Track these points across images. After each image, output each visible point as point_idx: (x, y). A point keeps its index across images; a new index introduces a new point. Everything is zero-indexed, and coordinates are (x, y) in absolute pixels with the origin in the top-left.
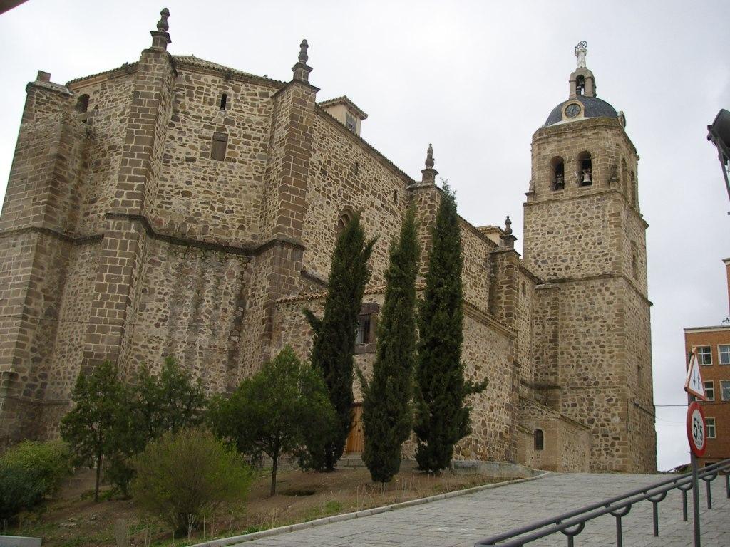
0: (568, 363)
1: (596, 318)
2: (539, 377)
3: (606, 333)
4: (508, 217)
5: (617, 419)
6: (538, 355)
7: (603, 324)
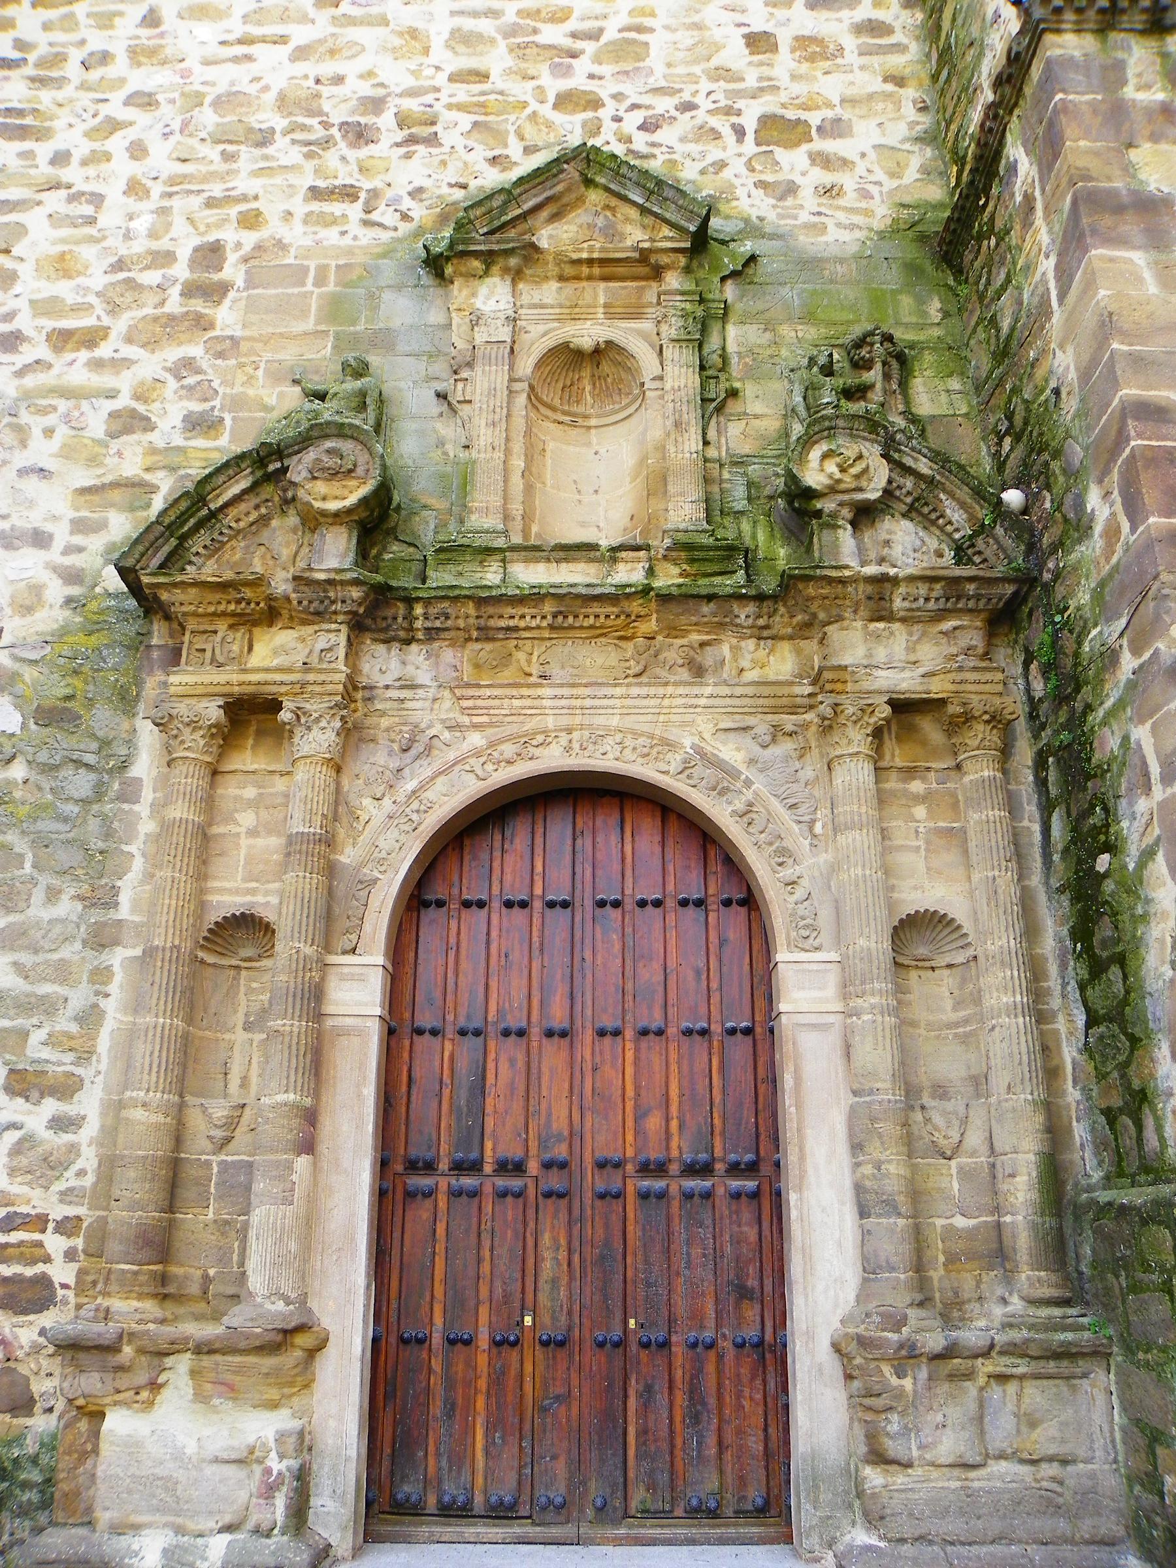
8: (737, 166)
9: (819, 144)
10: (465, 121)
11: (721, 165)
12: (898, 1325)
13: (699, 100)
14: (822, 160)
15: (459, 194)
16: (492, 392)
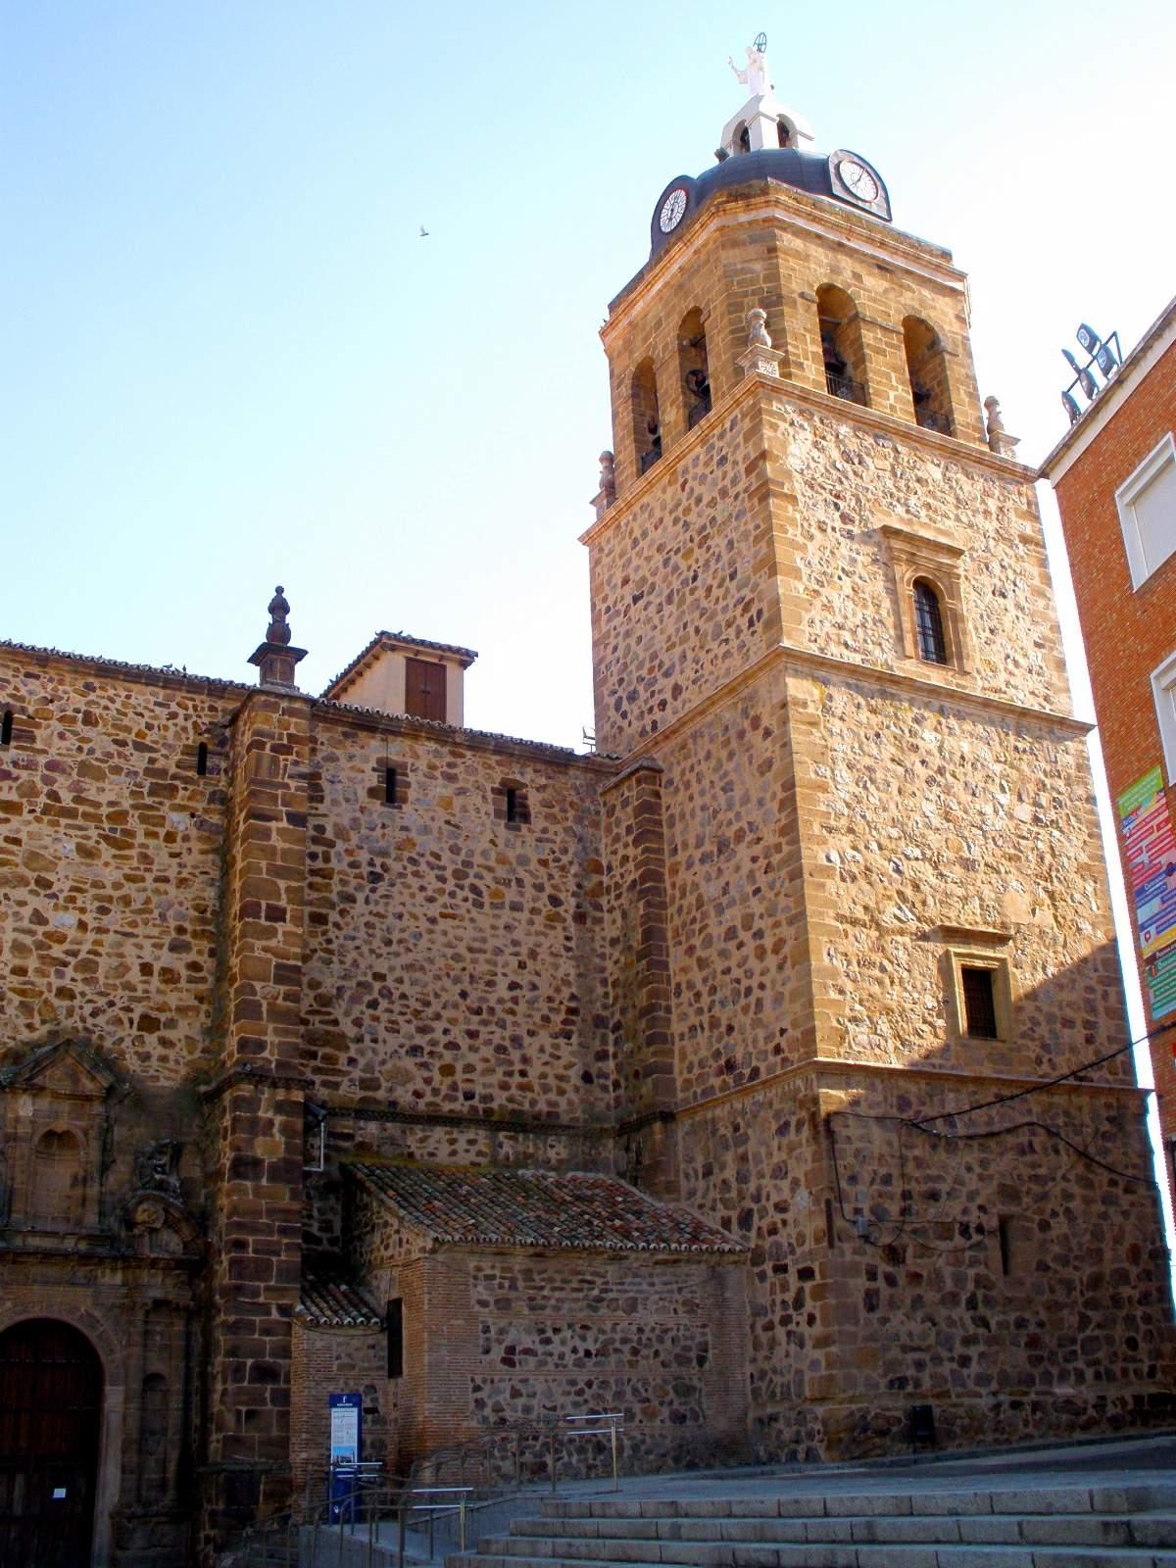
0: (694, 1020)
1: (739, 836)
2: (621, 1091)
3: (762, 880)
4: (280, 590)
5: (802, 1200)
6: (617, 1016)
7: (757, 850)
8: (128, 1042)
9: (164, 1033)
10: (17, 999)
11: (122, 1040)
12: (130, 1507)
13: (116, 1000)
14: (165, 1042)
15: (12, 1044)
16: (22, 1157)
